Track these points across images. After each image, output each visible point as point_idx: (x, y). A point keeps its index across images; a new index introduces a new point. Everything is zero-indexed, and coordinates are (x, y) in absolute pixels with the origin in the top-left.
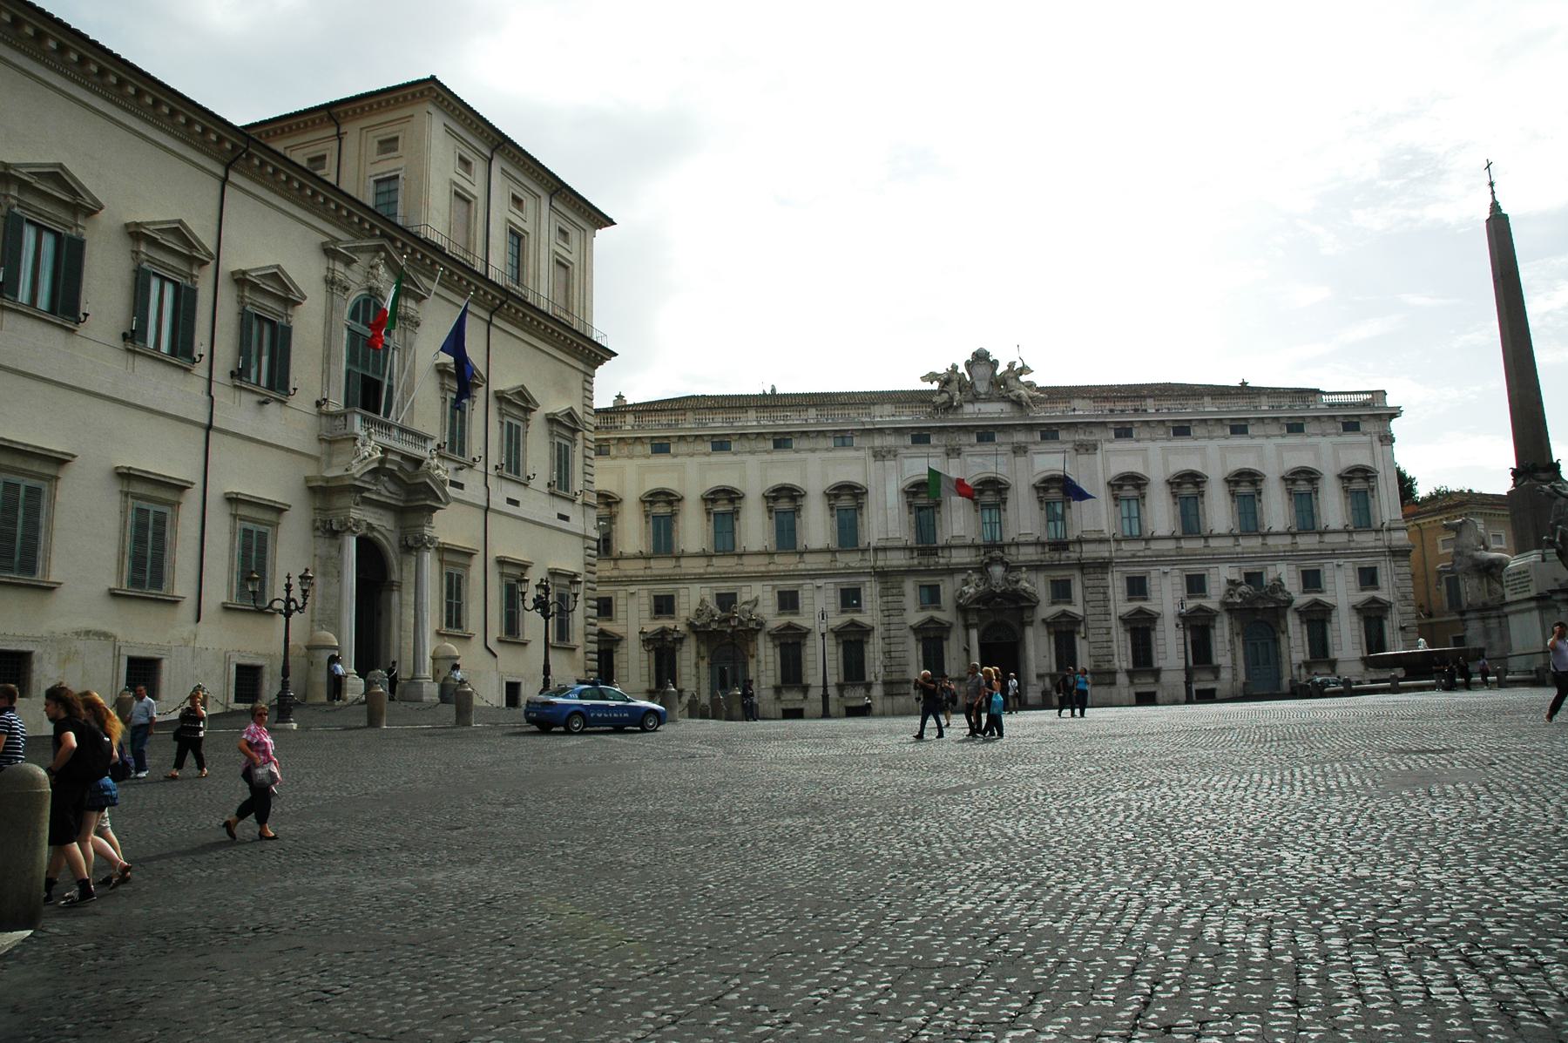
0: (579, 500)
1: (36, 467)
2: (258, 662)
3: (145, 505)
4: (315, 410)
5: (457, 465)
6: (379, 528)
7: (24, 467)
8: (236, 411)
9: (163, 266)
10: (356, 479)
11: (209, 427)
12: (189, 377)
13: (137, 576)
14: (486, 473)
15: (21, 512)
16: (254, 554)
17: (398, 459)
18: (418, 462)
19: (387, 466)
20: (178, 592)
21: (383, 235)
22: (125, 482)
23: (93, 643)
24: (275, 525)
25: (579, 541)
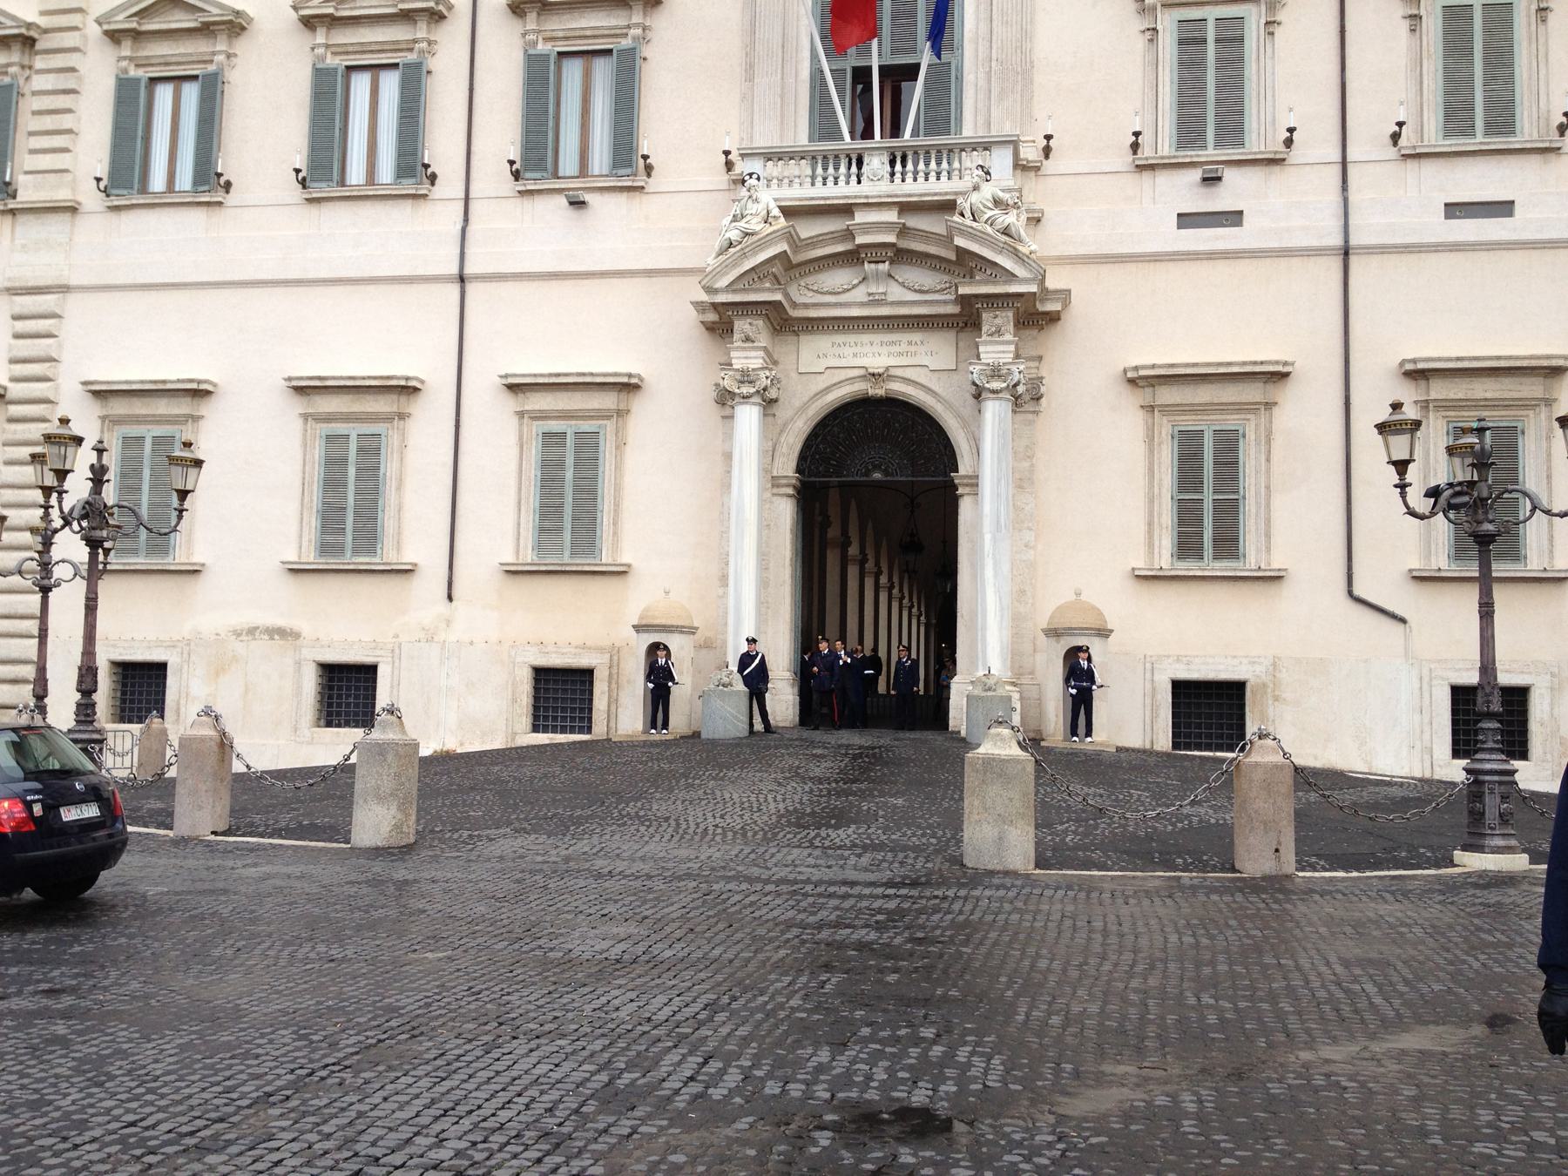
1: (162, 407)
2: (583, 662)
3: (340, 428)
4: (722, 179)
5: (1196, 175)
6: (908, 373)
7: (144, 411)
9: (364, 49)
10: (716, 291)
11: (462, 279)
12: (424, 208)
13: (329, 538)
14: (1344, 163)
15: (146, 473)
16: (569, 474)
17: (891, 216)
18: (948, 206)
19: (860, 240)
20: (408, 557)
22: (304, 399)
23: (262, 645)
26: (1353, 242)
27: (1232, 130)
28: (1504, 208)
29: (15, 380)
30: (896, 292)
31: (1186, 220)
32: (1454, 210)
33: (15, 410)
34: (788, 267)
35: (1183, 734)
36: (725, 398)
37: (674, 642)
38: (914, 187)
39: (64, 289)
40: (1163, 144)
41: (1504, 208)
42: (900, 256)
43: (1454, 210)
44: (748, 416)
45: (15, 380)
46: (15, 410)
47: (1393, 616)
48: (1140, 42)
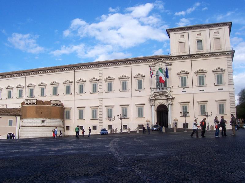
0: (227, 84)
4: (150, 89)
8: (137, 93)
18: (166, 92)
25: (228, 92)
27: (185, 85)
28: (203, 90)
30: (163, 97)
31: (183, 91)
33: (100, 108)
34: (154, 96)
35: (184, 127)
36: (151, 106)
37: (149, 123)
39: (102, 99)
42: (163, 95)
44: (153, 107)
46: (100, 108)
48: (179, 79)
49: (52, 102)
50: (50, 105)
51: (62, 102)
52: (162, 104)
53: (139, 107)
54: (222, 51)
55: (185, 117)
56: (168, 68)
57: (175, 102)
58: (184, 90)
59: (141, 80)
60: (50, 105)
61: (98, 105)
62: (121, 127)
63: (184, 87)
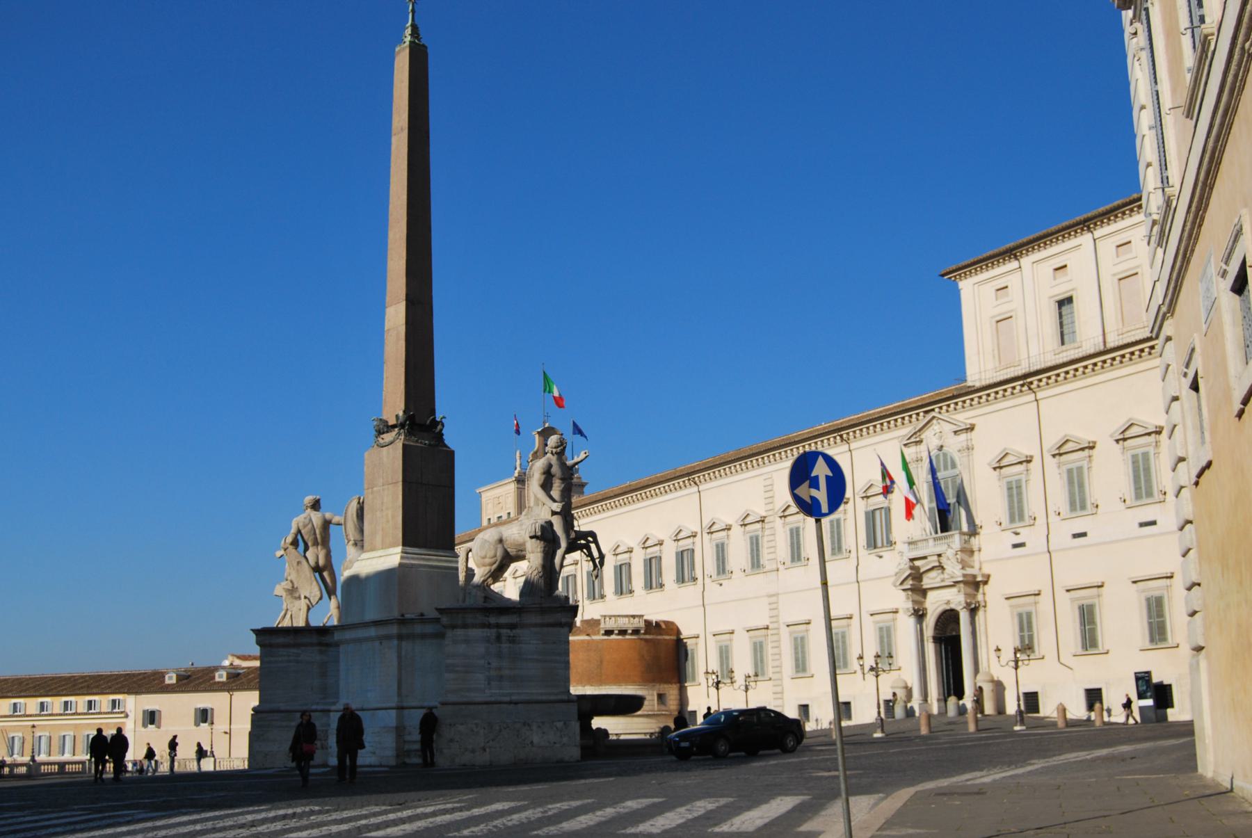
21: (926, 412)
24: (894, 620)
26: (1050, 550)
29: (771, 623)
31: (1015, 546)
32: (1076, 536)
33: (770, 632)
38: (938, 550)
39: (777, 595)
40: (1005, 520)
41: (1084, 535)
43: (1076, 536)
45: (771, 623)
47: (1069, 667)
49: (606, 625)
50: (598, 633)
51: (645, 618)
52: (948, 608)
53: (881, 625)
54: (1080, 355)
55: (877, 676)
56: (908, 459)
57: (991, 595)
58: (1018, 540)
59: (1016, 478)
60: (595, 634)
61: (766, 622)
62: (1019, 700)
63: (1018, 525)
